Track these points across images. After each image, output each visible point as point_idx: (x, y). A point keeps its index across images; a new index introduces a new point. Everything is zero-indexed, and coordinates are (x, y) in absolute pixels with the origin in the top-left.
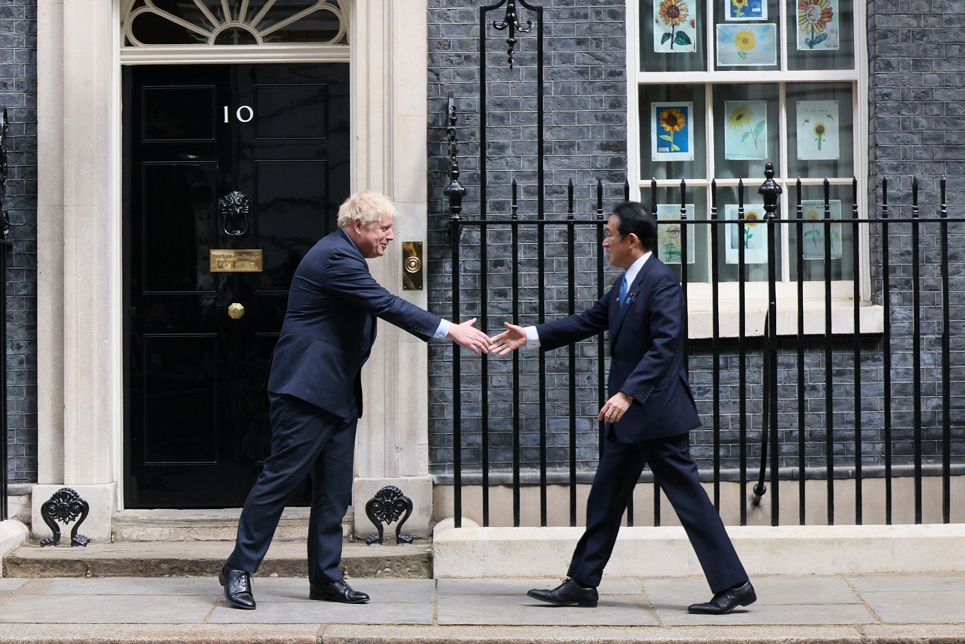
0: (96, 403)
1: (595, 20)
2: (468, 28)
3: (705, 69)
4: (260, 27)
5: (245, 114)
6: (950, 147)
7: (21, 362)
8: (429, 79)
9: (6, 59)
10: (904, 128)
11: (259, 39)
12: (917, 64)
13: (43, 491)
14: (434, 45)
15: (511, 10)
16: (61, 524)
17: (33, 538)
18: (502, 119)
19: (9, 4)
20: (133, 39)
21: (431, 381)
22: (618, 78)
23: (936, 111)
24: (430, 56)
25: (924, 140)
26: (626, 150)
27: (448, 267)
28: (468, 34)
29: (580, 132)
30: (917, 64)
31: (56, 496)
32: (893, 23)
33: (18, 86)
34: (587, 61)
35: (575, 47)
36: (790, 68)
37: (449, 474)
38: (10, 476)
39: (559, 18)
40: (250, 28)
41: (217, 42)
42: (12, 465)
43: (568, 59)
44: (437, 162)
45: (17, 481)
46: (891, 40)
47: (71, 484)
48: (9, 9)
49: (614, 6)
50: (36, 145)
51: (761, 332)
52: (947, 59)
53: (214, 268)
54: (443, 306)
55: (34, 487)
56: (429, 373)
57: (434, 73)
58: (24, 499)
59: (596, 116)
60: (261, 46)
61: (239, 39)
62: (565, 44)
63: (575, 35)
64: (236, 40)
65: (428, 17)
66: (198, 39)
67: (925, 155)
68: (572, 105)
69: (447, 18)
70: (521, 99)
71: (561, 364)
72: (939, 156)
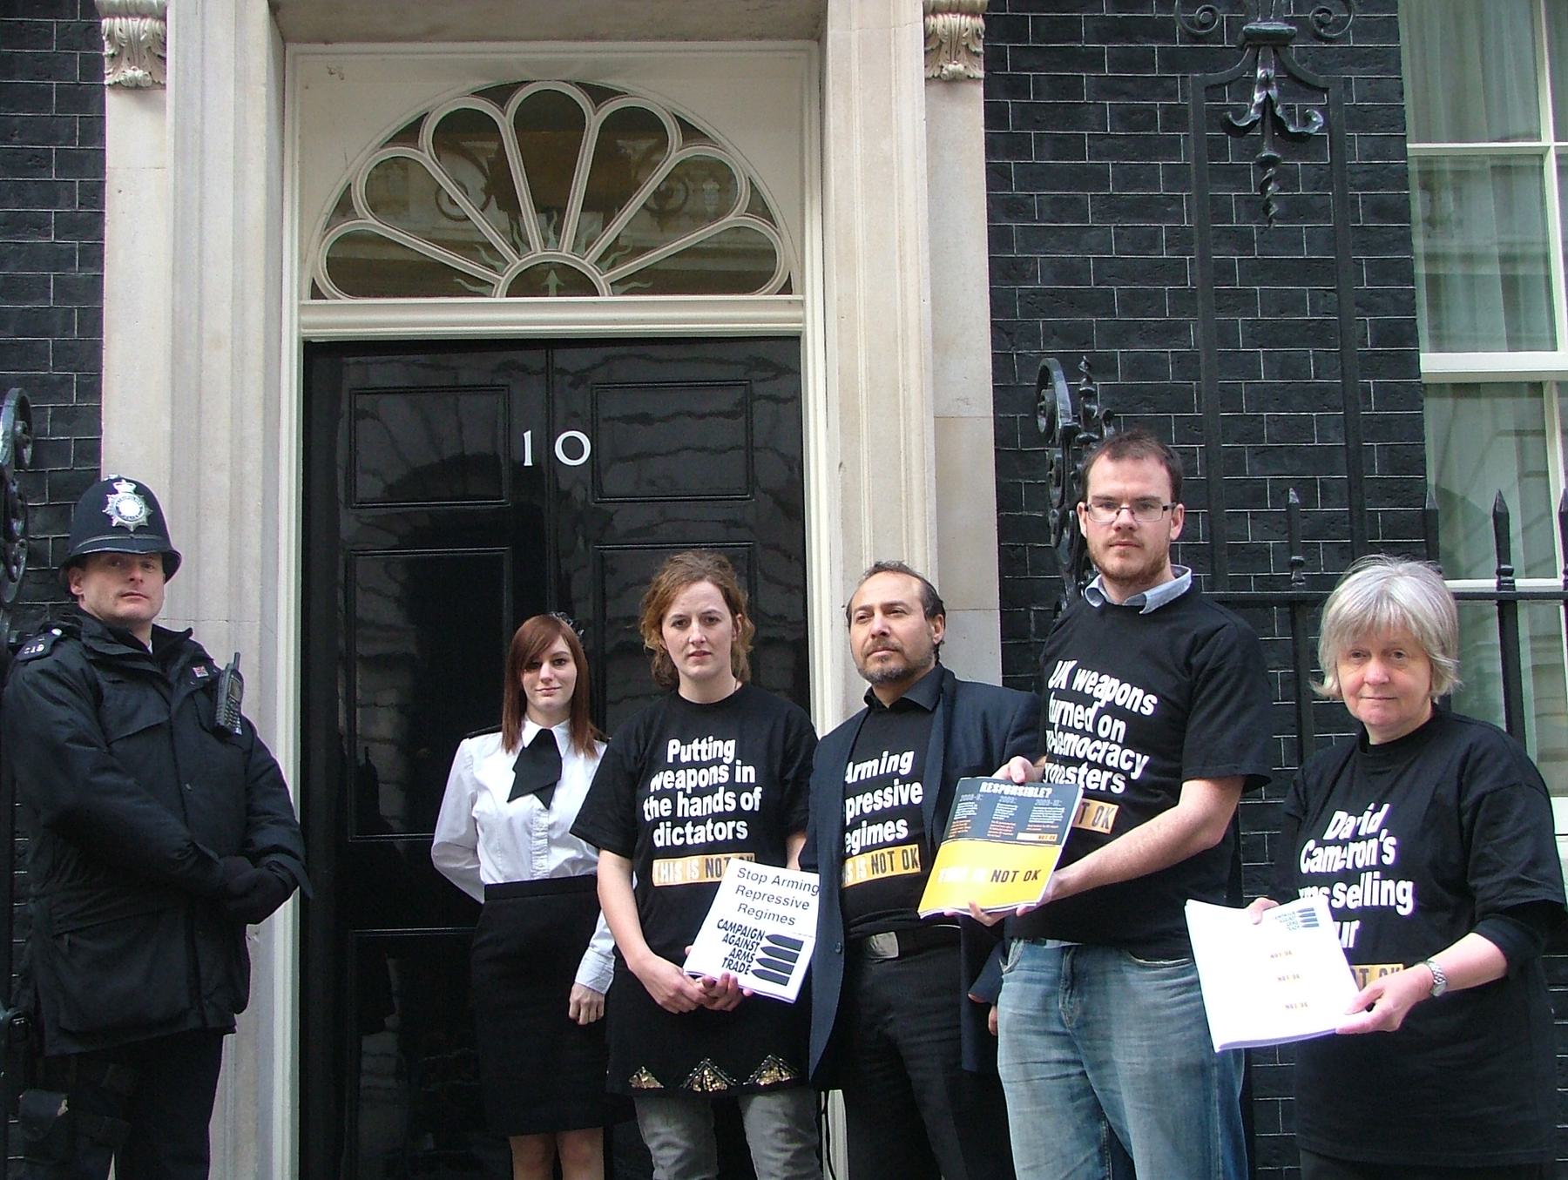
4: (608, 258)
5: (573, 448)
8: (995, 343)
9: (30, 297)
14: (1002, 271)
20: (325, 284)
40: (586, 264)
57: (1001, 332)
61: (558, 287)
64: (552, 288)
66: (472, 288)
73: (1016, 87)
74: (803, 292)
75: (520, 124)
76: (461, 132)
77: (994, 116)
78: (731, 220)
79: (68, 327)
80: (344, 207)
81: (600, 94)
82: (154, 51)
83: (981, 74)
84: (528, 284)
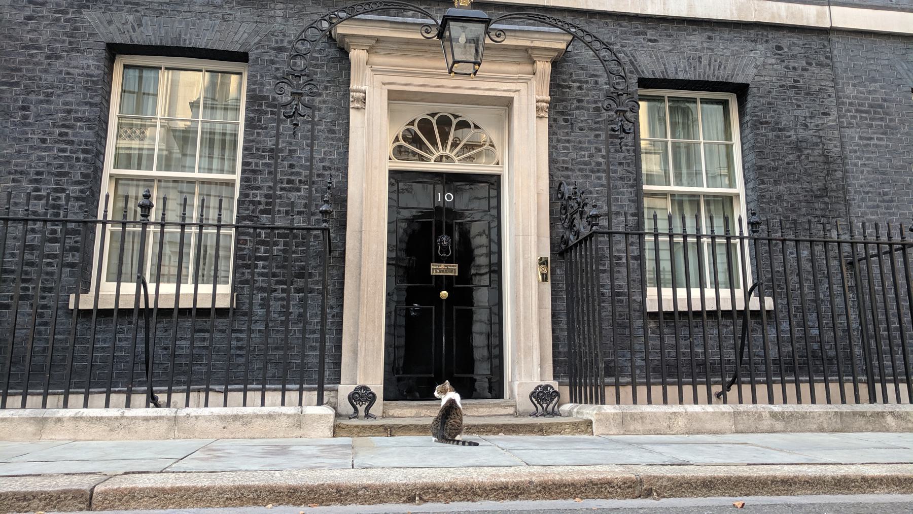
2: (567, 155)
4: (458, 155)
5: (449, 197)
7: (333, 316)
13: (345, 389)
14: (552, 161)
16: (358, 406)
17: (338, 415)
19: (334, 128)
29: (622, 207)
30: (776, 183)
32: (763, 164)
37: (567, 380)
40: (452, 155)
42: (326, 373)
43: (615, 172)
46: (763, 171)
47: (360, 383)
50: (346, 201)
53: (433, 273)
57: (551, 176)
58: (332, 393)
68: (618, 194)
69: (557, 149)
70: (593, 190)
74: (503, 164)
76: (425, 125)
77: (550, 126)
81: (456, 117)
84: (440, 159)
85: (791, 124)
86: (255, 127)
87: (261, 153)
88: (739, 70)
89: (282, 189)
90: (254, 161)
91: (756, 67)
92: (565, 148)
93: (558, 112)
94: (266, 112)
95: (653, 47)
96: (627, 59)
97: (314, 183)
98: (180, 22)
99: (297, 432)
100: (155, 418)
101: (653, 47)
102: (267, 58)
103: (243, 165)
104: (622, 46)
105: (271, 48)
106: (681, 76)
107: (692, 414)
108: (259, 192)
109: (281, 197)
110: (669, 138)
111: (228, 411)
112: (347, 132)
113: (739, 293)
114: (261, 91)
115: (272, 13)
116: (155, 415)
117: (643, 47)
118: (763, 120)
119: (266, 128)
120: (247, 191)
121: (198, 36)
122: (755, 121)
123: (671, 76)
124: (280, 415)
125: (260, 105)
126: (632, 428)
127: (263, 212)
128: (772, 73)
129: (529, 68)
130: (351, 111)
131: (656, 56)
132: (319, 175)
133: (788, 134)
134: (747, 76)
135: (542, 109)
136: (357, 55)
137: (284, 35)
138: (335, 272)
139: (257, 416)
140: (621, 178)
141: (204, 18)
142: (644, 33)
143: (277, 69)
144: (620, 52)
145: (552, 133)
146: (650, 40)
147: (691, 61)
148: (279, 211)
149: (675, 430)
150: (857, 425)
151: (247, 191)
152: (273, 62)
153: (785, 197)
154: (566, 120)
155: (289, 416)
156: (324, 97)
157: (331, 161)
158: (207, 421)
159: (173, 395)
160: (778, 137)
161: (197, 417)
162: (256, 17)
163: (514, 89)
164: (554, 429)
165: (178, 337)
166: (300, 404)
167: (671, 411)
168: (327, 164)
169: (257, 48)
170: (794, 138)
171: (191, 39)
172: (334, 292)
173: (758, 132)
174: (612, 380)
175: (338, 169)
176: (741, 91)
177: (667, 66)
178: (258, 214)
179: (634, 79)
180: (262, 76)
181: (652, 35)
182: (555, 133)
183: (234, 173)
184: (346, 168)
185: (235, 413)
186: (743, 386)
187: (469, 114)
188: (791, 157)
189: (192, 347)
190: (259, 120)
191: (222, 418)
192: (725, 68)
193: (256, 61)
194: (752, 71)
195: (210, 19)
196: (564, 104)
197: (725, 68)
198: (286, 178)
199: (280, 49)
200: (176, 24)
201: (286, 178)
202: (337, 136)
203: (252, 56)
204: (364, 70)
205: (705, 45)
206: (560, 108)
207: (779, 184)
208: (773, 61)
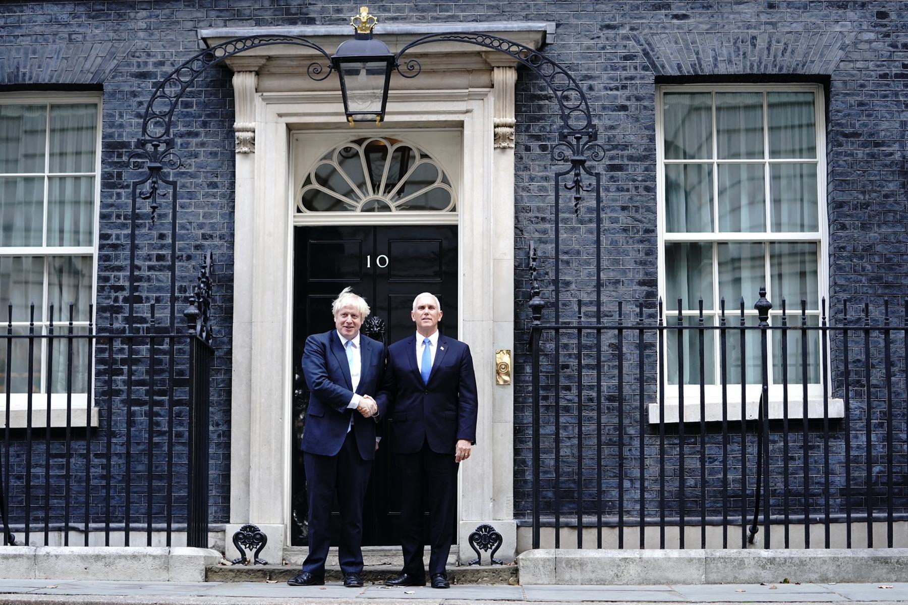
0: (274, 465)
1: (635, 193)
2: (543, 198)
3: (713, 231)
5: (383, 261)
6: (888, 286)
7: (219, 436)
8: (516, 234)
9: (212, 218)
10: (855, 271)
11: (393, 208)
12: (864, 227)
13: (233, 528)
14: (519, 210)
15: (577, 175)
16: (247, 551)
18: (567, 263)
19: (215, 180)
20: (302, 208)
21: (517, 452)
22: (651, 235)
23: (877, 259)
24: (517, 218)
25: (870, 280)
26: (657, 286)
27: (528, 369)
28: (544, 201)
29: (624, 272)
31: (244, 529)
33: (220, 238)
34: (629, 222)
35: (620, 211)
36: (772, 231)
37: (530, 520)
38: (210, 518)
39: (609, 191)
40: (387, 199)
41: (362, 211)
42: (212, 510)
43: (614, 221)
44: (521, 293)
45: (215, 522)
46: (845, 209)
47: (254, 522)
48: (216, 183)
49: (648, 183)
51: (756, 417)
52: (885, 223)
54: (525, 398)
55: (227, 525)
56: (514, 446)
57: (519, 230)
58: (220, 534)
59: (635, 261)
60: (395, 212)
62: (613, 210)
63: (620, 204)
65: (515, 190)
67: (870, 291)
69: (529, 191)
70: (581, 249)
71: (610, 440)
72: (880, 292)
73: (528, 149)
75: (367, 151)
76: (347, 155)
77: (518, 158)
78: (435, 185)
79: (223, 227)
80: (308, 181)
81: (393, 142)
82: (252, 142)
83: (513, 146)
84: (368, 208)
85: (896, 135)
86: (113, 186)
87: (122, 220)
88: (815, 54)
89: (151, 268)
90: (114, 232)
91: (843, 48)
92: (542, 189)
93: (532, 136)
94: (127, 165)
95: (679, 27)
96: (639, 49)
97: (189, 258)
98: (18, 51)
99: (165, 575)
100: (15, 557)
101: (679, 27)
102: (127, 89)
103: (100, 238)
104: (632, 29)
105: (132, 75)
106: (722, 69)
107: (648, 561)
108: (121, 274)
109: (149, 279)
110: (715, 160)
111: (90, 550)
112: (232, 184)
113: (815, 391)
114: (120, 135)
115: (132, 25)
116: (14, 553)
117: (664, 28)
118: (848, 130)
119: (128, 186)
120: (107, 273)
121: (39, 67)
122: (837, 133)
123: (707, 71)
124: (145, 556)
125: (120, 155)
126: (567, 577)
127: (125, 300)
128: (868, 55)
129: (484, 79)
130: (238, 157)
131: (685, 41)
132: (197, 247)
133: (890, 150)
134: (828, 63)
135: (505, 137)
136: (242, 82)
137: (149, 55)
138: (220, 377)
139: (120, 557)
140: (625, 230)
141: (46, 40)
142: (668, 6)
143: (140, 103)
144: (628, 38)
145: (520, 166)
146: (676, 17)
147: (740, 44)
148: (147, 298)
149: (626, 578)
150: (875, 573)
151: (107, 273)
152: (134, 94)
153: (878, 248)
154: (544, 148)
155: (155, 557)
156: (202, 138)
157: (213, 226)
158: (67, 561)
159: (31, 534)
160: (873, 156)
161: (57, 556)
162: (111, 34)
163: (464, 109)
164: (469, 577)
165: (33, 463)
166: (169, 544)
167: (621, 556)
168: (207, 231)
169: (114, 77)
170: (897, 156)
171: (31, 73)
172: (219, 403)
173: (840, 149)
174: (594, 519)
175: (222, 237)
176: (824, 81)
177: (701, 55)
178: (121, 304)
179: (650, 76)
180: (121, 116)
181: (680, 8)
182: (526, 168)
183: (90, 243)
184: (232, 235)
185: (96, 553)
186: (875, 525)
187: (408, 139)
188: (892, 186)
189: (47, 476)
190: (119, 175)
191: (84, 558)
192: (793, 52)
193: (113, 95)
194: (836, 54)
195: (54, 41)
196: (541, 123)
197: (793, 52)
198: (155, 252)
199: (143, 76)
200: (13, 54)
201: (155, 252)
202: (219, 191)
203: (108, 88)
204: (252, 100)
205: (763, 18)
206: (534, 130)
207: (870, 229)
208: (872, 36)
